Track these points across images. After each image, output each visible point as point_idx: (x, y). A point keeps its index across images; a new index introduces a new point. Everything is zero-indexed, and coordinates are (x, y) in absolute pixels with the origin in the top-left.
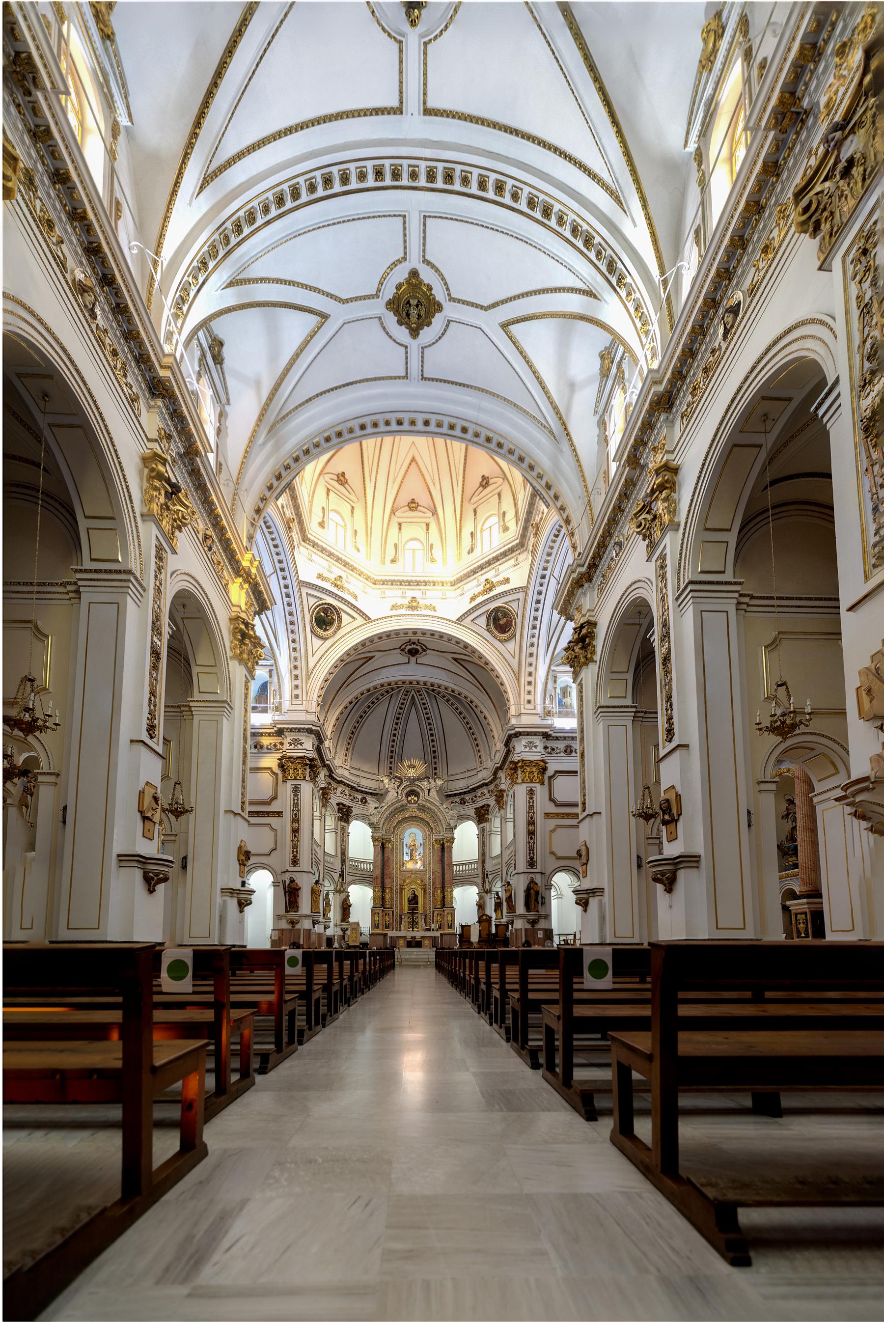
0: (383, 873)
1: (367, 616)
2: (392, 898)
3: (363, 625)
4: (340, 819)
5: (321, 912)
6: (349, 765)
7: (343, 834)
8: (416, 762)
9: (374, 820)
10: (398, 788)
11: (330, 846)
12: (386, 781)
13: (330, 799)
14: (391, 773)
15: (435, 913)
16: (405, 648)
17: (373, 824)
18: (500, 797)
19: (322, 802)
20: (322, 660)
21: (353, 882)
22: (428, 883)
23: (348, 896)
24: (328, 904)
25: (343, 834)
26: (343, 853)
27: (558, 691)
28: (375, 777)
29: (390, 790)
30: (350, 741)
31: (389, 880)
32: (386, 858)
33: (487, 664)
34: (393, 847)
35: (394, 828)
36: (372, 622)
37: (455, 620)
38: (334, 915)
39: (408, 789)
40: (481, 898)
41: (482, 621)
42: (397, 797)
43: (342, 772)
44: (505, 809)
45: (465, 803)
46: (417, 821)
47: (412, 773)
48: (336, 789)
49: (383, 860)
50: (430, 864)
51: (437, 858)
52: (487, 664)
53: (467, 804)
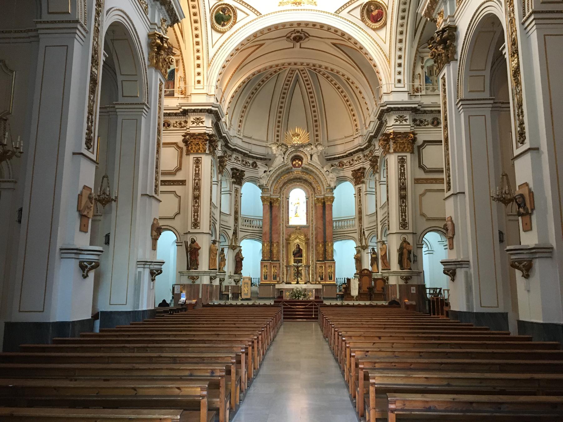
0: (271, 229)
1: (258, 12)
2: (278, 252)
3: (255, 20)
4: (234, 183)
5: (218, 268)
6: (242, 134)
7: (236, 195)
9: (263, 182)
10: (284, 154)
11: (226, 206)
12: (274, 148)
13: (225, 165)
14: (278, 140)
15: (318, 266)
16: (290, 36)
17: (262, 186)
18: (374, 162)
19: (219, 169)
20: (220, 51)
21: (245, 238)
23: (240, 250)
24: (223, 260)
25: (236, 195)
26: (236, 212)
27: (425, 70)
28: (264, 144)
29: (277, 155)
30: (243, 114)
31: (277, 235)
32: (273, 216)
33: (362, 49)
34: (280, 206)
35: (281, 188)
36: (262, 17)
37: (333, 13)
38: (229, 267)
39: (293, 155)
40: (358, 252)
41: (357, 13)
42: (283, 162)
43: (235, 142)
44: (379, 173)
45: (343, 165)
47: (296, 141)
48: (231, 156)
49: (271, 217)
50: (312, 220)
51: (320, 215)
52: (361, 48)
53: (345, 167)
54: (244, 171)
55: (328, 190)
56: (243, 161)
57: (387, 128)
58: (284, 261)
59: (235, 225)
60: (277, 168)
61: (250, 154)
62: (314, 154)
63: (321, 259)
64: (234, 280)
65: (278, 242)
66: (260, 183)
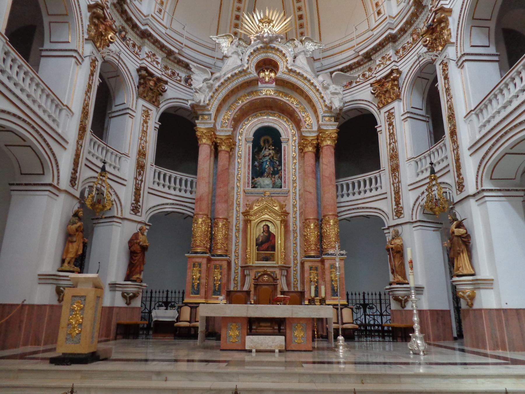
0: (213, 193)
2: (227, 238)
8: (275, 16)
15: (307, 266)
22: (291, 212)
31: (224, 206)
32: (220, 168)
42: (242, 65)
46: (274, 115)
48: (140, 48)
54: (166, 83)
55: (327, 119)
56: (166, 68)
58: (238, 258)
59: (136, 179)
60: (229, 75)
62: (300, 53)
63: (312, 253)
64: (123, 296)
65: (227, 219)
66: (193, 100)
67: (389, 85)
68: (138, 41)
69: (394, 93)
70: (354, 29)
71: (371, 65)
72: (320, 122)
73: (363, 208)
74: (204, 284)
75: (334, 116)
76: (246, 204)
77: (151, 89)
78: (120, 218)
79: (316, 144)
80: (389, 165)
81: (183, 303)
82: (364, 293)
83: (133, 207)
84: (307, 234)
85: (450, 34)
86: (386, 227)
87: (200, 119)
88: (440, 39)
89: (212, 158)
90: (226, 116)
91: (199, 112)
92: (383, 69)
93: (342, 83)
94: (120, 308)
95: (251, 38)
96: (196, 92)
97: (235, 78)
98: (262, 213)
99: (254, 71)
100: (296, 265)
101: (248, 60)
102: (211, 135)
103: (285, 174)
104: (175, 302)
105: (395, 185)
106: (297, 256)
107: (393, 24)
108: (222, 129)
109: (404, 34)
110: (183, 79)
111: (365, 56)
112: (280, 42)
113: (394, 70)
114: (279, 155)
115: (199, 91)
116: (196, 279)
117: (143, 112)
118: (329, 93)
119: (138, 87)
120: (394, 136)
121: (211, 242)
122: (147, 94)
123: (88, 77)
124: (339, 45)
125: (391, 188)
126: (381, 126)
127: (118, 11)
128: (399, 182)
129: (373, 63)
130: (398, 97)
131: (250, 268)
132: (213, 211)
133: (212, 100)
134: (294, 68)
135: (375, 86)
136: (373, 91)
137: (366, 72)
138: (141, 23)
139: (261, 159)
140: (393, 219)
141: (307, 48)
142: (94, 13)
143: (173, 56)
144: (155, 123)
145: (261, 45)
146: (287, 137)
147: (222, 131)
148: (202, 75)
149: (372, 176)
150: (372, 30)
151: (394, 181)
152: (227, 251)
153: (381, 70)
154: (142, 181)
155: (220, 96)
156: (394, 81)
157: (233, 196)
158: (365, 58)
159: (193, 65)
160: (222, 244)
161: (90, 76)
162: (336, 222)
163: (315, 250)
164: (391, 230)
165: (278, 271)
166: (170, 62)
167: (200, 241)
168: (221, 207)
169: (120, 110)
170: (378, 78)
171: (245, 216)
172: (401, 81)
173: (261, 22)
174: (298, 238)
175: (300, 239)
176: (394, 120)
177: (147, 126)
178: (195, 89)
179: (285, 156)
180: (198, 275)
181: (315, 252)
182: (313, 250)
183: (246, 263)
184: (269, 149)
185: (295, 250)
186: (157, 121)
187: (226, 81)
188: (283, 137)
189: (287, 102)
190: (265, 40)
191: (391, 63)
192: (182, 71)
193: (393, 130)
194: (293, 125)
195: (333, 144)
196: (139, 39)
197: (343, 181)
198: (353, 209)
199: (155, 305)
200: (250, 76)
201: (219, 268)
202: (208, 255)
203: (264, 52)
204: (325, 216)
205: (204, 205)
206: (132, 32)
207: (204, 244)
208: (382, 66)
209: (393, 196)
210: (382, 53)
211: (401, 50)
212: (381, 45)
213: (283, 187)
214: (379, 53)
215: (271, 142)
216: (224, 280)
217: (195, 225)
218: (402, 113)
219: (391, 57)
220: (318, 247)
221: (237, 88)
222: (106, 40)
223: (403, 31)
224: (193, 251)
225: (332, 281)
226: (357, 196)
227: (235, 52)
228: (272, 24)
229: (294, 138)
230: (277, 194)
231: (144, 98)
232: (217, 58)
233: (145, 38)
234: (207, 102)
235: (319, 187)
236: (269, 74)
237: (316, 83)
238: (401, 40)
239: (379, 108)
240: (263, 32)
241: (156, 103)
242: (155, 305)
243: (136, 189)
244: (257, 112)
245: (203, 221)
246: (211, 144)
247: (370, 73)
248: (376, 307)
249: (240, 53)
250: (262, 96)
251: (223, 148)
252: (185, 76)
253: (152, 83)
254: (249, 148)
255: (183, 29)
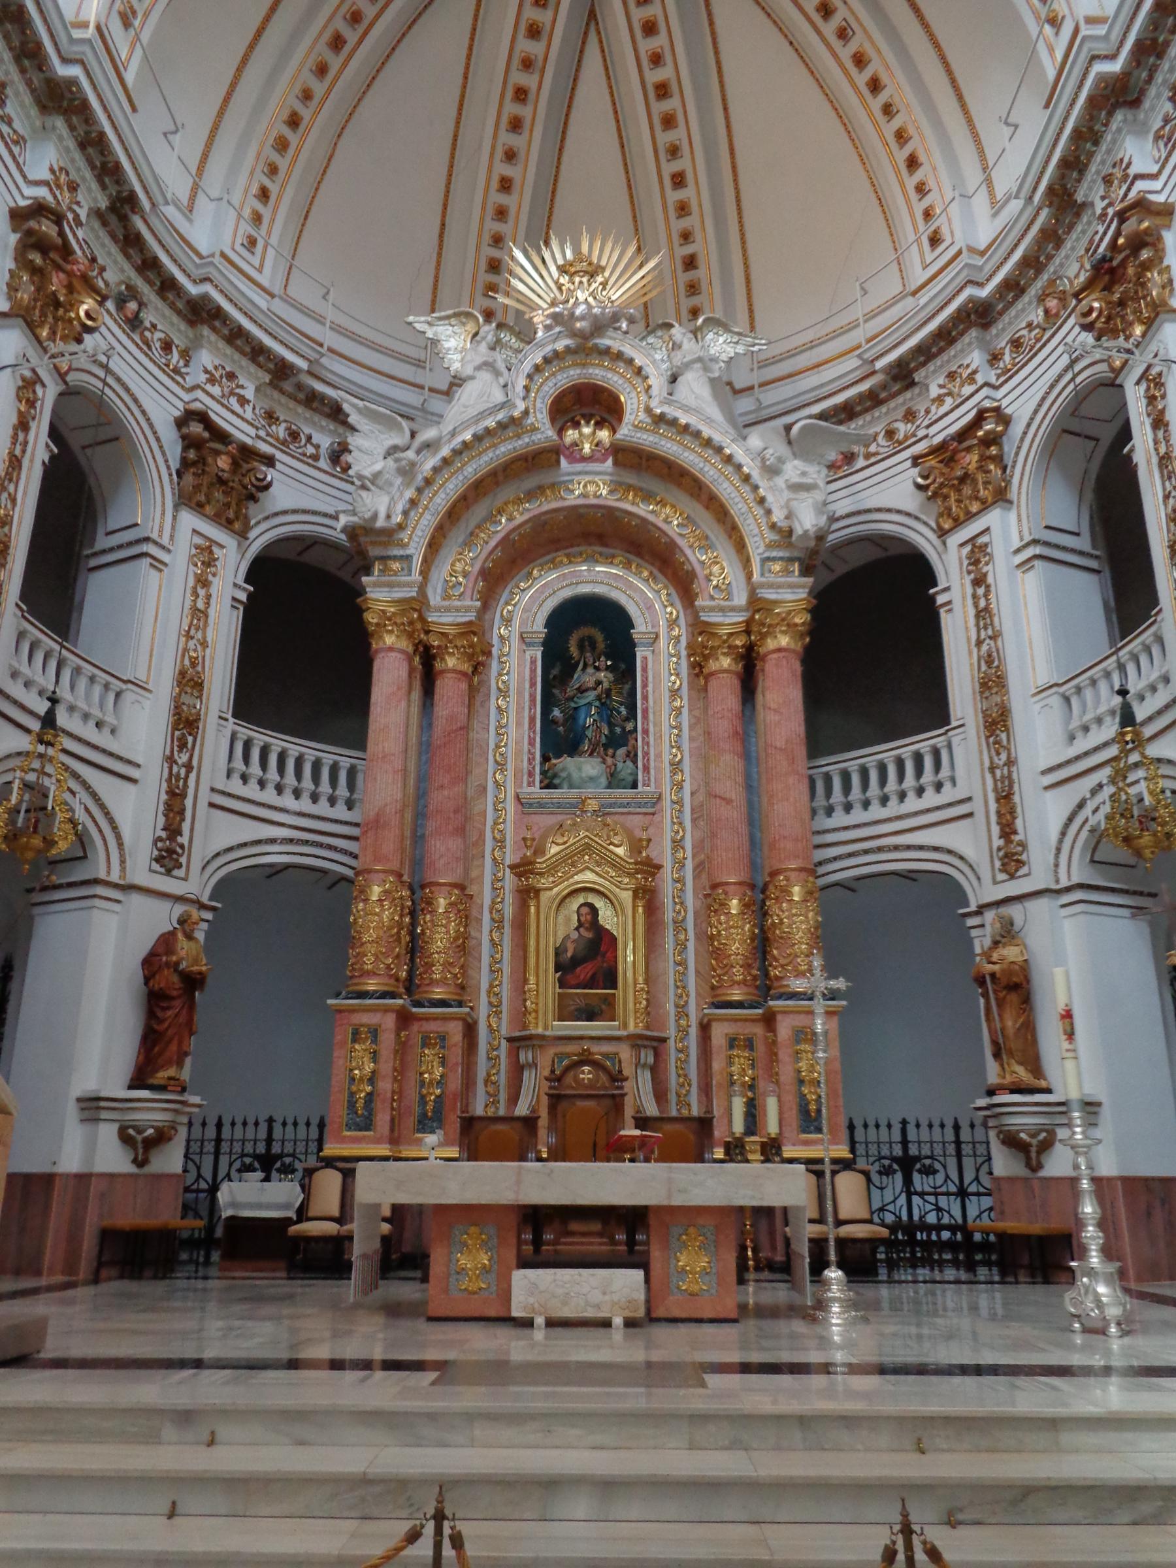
2: (463, 946)
8: (607, 254)
15: (719, 1034)
22: (668, 863)
46: (609, 560)
48: (186, 355)
54: (270, 461)
55: (777, 567)
56: (271, 417)
57: (1140, 185)
58: (498, 1013)
59: (170, 760)
60: (468, 436)
61: (320, 387)
62: (687, 366)
63: (736, 995)
64: (125, 1138)
66: (354, 513)
67: (971, 460)
68: (179, 333)
69: (989, 483)
70: (859, 293)
71: (912, 399)
72: (756, 577)
73: (896, 848)
74: (389, 1095)
75: (799, 559)
76: (524, 839)
77: (221, 482)
78: (116, 886)
79: (743, 646)
80: (976, 711)
81: (320, 1159)
82: (904, 1123)
83: (160, 850)
84: (719, 932)
85: (1171, 281)
86: (973, 907)
87: (376, 573)
88: (1137, 300)
89: (416, 695)
90: (458, 564)
91: (373, 551)
92: (952, 411)
93: (822, 456)
94: (112, 1176)
95: (535, 320)
96: (364, 487)
97: (487, 443)
98: (573, 865)
99: (547, 421)
100: (684, 1032)
101: (527, 389)
102: (411, 623)
103: (648, 744)
104: (293, 1155)
105: (998, 773)
106: (687, 1002)
107: (981, 268)
108: (446, 603)
109: (1016, 298)
110: (323, 451)
111: (895, 371)
112: (626, 333)
113: (987, 410)
114: (627, 687)
115: (373, 483)
116: (361, 1079)
117: (194, 551)
118: (784, 486)
119: (179, 474)
120: (991, 617)
121: (412, 960)
122: (207, 495)
123: (10, 432)
124: (812, 345)
125: (984, 784)
126: (947, 589)
127: (113, 237)
128: (1010, 762)
129: (920, 394)
130: (1001, 496)
131: (535, 1042)
132: (418, 862)
133: (412, 513)
134: (671, 412)
135: (928, 464)
136: (920, 480)
137: (896, 425)
138: (189, 276)
139: (571, 699)
140: (995, 882)
141: (712, 352)
142: (29, 233)
143: (293, 380)
144: (235, 585)
145: (567, 342)
146: (653, 627)
147: (448, 610)
148: (382, 436)
149: (924, 747)
150: (914, 293)
151: (996, 759)
152: (462, 987)
153: (946, 414)
154: (189, 767)
155: (438, 500)
156: (988, 447)
157: (484, 813)
158: (895, 379)
159: (354, 406)
160: (448, 965)
161: (15, 428)
162: (810, 893)
163: (744, 982)
164: (989, 916)
165: (625, 1053)
166: (284, 399)
167: (376, 956)
168: (443, 849)
169: (120, 547)
170: (937, 440)
171: (519, 875)
172: (1009, 448)
173: (566, 272)
174: (691, 945)
175: (696, 949)
176: (990, 567)
177: (209, 597)
178: (360, 477)
179: (645, 686)
180: (369, 1067)
181: (745, 990)
182: (739, 983)
183: (525, 1027)
184: (597, 669)
185: (681, 985)
186: (240, 580)
187: (457, 453)
188: (640, 627)
189: (651, 518)
190: (578, 325)
191: (977, 391)
192: (322, 429)
193: (987, 600)
194: (672, 590)
195: (799, 647)
196: (183, 326)
197: (833, 764)
198: (866, 852)
199: (231, 1165)
200: (533, 437)
201: (436, 1044)
202: (400, 1001)
203: (575, 365)
204: (774, 874)
205: (390, 843)
206: (160, 303)
207: (388, 967)
208: (949, 402)
209: (993, 806)
210: (948, 361)
211: (1007, 351)
212: (945, 337)
213: (640, 785)
214: (938, 362)
215: (601, 646)
216: (455, 1083)
217: (361, 905)
218: (1017, 544)
219: (975, 372)
220: (755, 972)
221: (493, 474)
222: (70, 320)
223: (1013, 288)
224: (350, 989)
225: (801, 1082)
226: (876, 812)
227: (486, 364)
228: (600, 279)
229: (676, 632)
230: (622, 805)
231: (199, 508)
232: (431, 390)
233: (203, 322)
234: (398, 518)
235: (755, 784)
236: (594, 433)
237: (740, 455)
238: (1006, 318)
239: (942, 533)
240: (572, 301)
241: (237, 526)
242: (231, 1165)
243: (171, 793)
244: (557, 550)
245: (386, 892)
246: (410, 649)
247: (909, 425)
248: (945, 1167)
249: (501, 366)
250: (572, 499)
251: (451, 662)
252: (332, 444)
253: (223, 462)
254: (533, 662)
255: (324, 297)
